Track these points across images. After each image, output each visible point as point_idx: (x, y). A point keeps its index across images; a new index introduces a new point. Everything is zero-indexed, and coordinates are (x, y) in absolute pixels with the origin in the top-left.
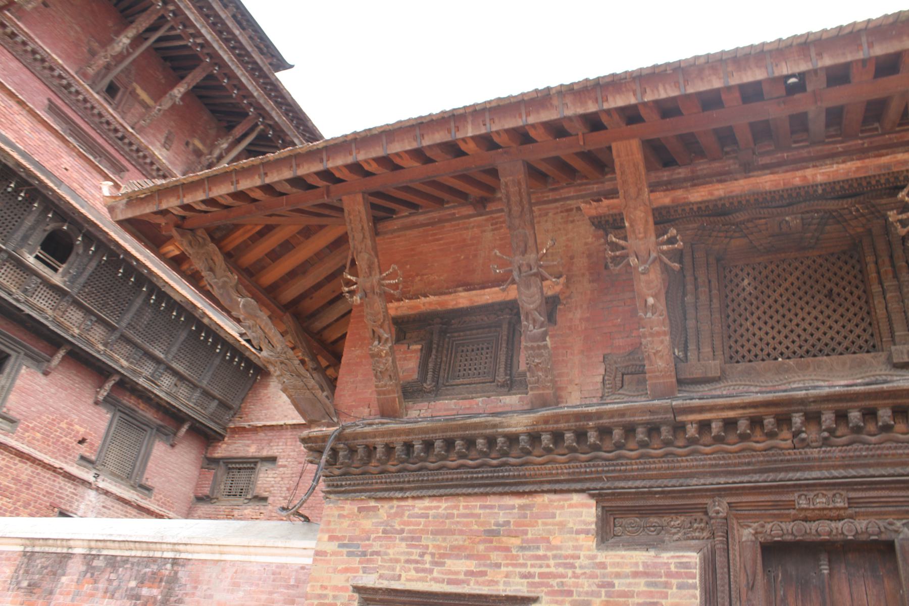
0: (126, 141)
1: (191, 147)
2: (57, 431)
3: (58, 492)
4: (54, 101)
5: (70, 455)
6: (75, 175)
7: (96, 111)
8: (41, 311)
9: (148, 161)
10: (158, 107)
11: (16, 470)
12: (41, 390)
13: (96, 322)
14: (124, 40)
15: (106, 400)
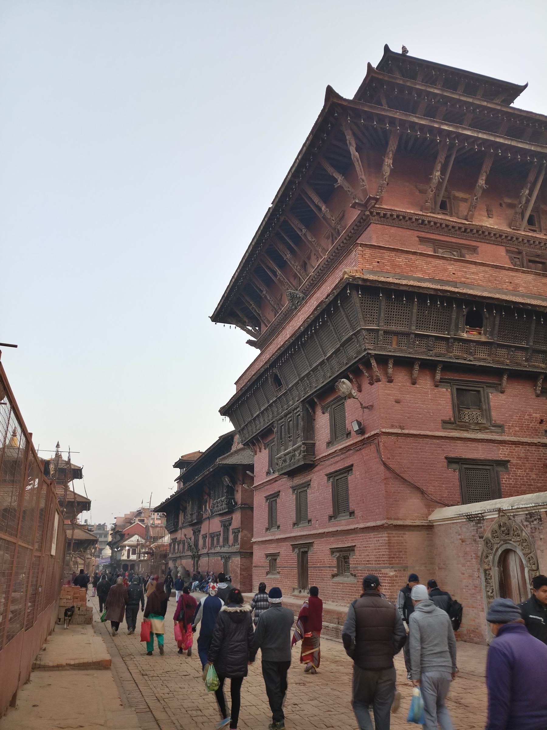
0: (469, 230)
1: (504, 205)
2: (525, 422)
3: (544, 456)
4: (420, 236)
5: (539, 433)
6: (460, 274)
7: (444, 226)
8: (484, 360)
9: (487, 233)
10: (475, 198)
11: (516, 452)
12: (505, 402)
13: (515, 350)
14: (438, 174)
15: (541, 392)
